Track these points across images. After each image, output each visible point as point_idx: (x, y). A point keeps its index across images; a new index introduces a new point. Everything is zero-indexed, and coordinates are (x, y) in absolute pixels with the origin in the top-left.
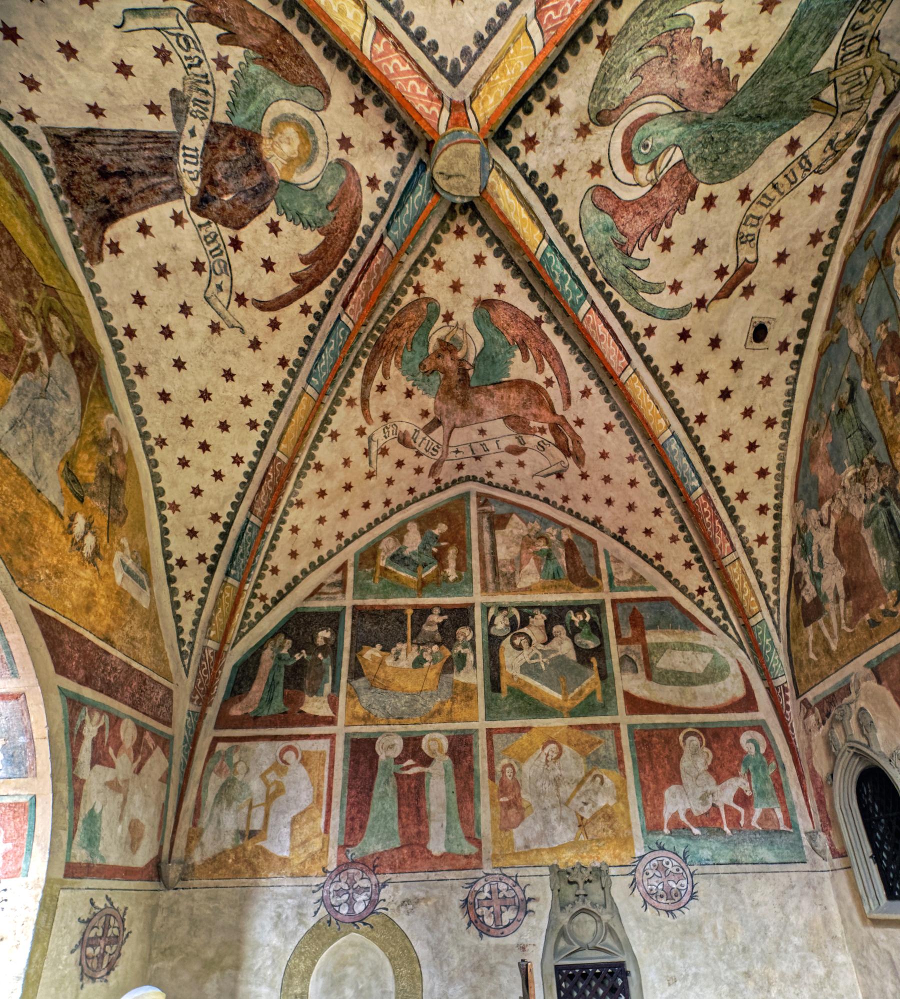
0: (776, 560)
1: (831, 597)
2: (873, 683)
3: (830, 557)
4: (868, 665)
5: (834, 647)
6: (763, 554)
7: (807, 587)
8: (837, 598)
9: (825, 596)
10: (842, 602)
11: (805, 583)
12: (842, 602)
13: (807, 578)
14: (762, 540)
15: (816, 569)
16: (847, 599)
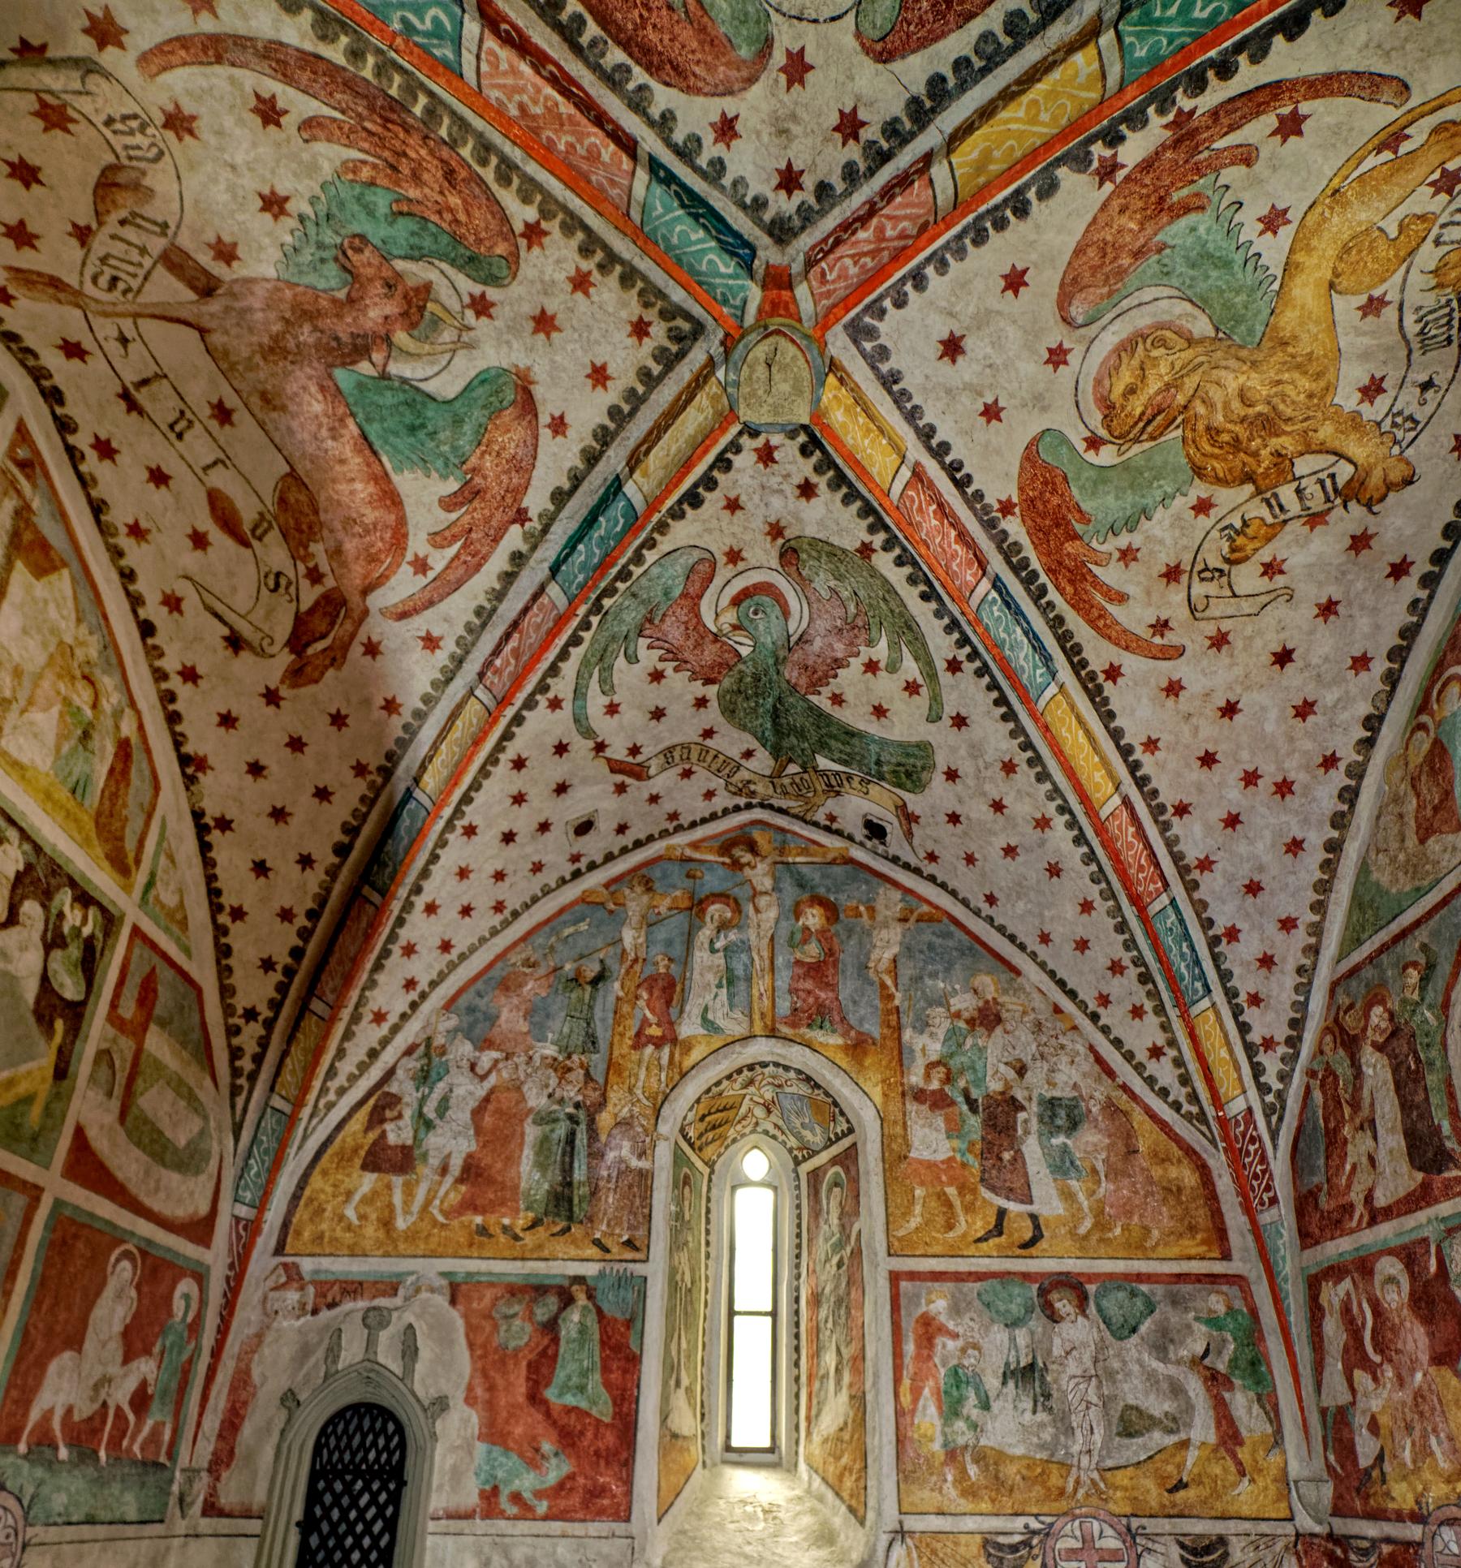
0: (373, 1054)
1: (434, 1161)
2: (441, 1301)
3: (461, 1115)
4: (443, 1274)
5: (401, 1224)
6: (369, 1034)
7: (401, 1123)
8: (444, 1170)
9: (425, 1156)
10: (449, 1180)
11: (400, 1116)
12: (449, 1180)
13: (408, 1113)
14: (379, 1017)
15: (430, 1111)
16: (460, 1180)
